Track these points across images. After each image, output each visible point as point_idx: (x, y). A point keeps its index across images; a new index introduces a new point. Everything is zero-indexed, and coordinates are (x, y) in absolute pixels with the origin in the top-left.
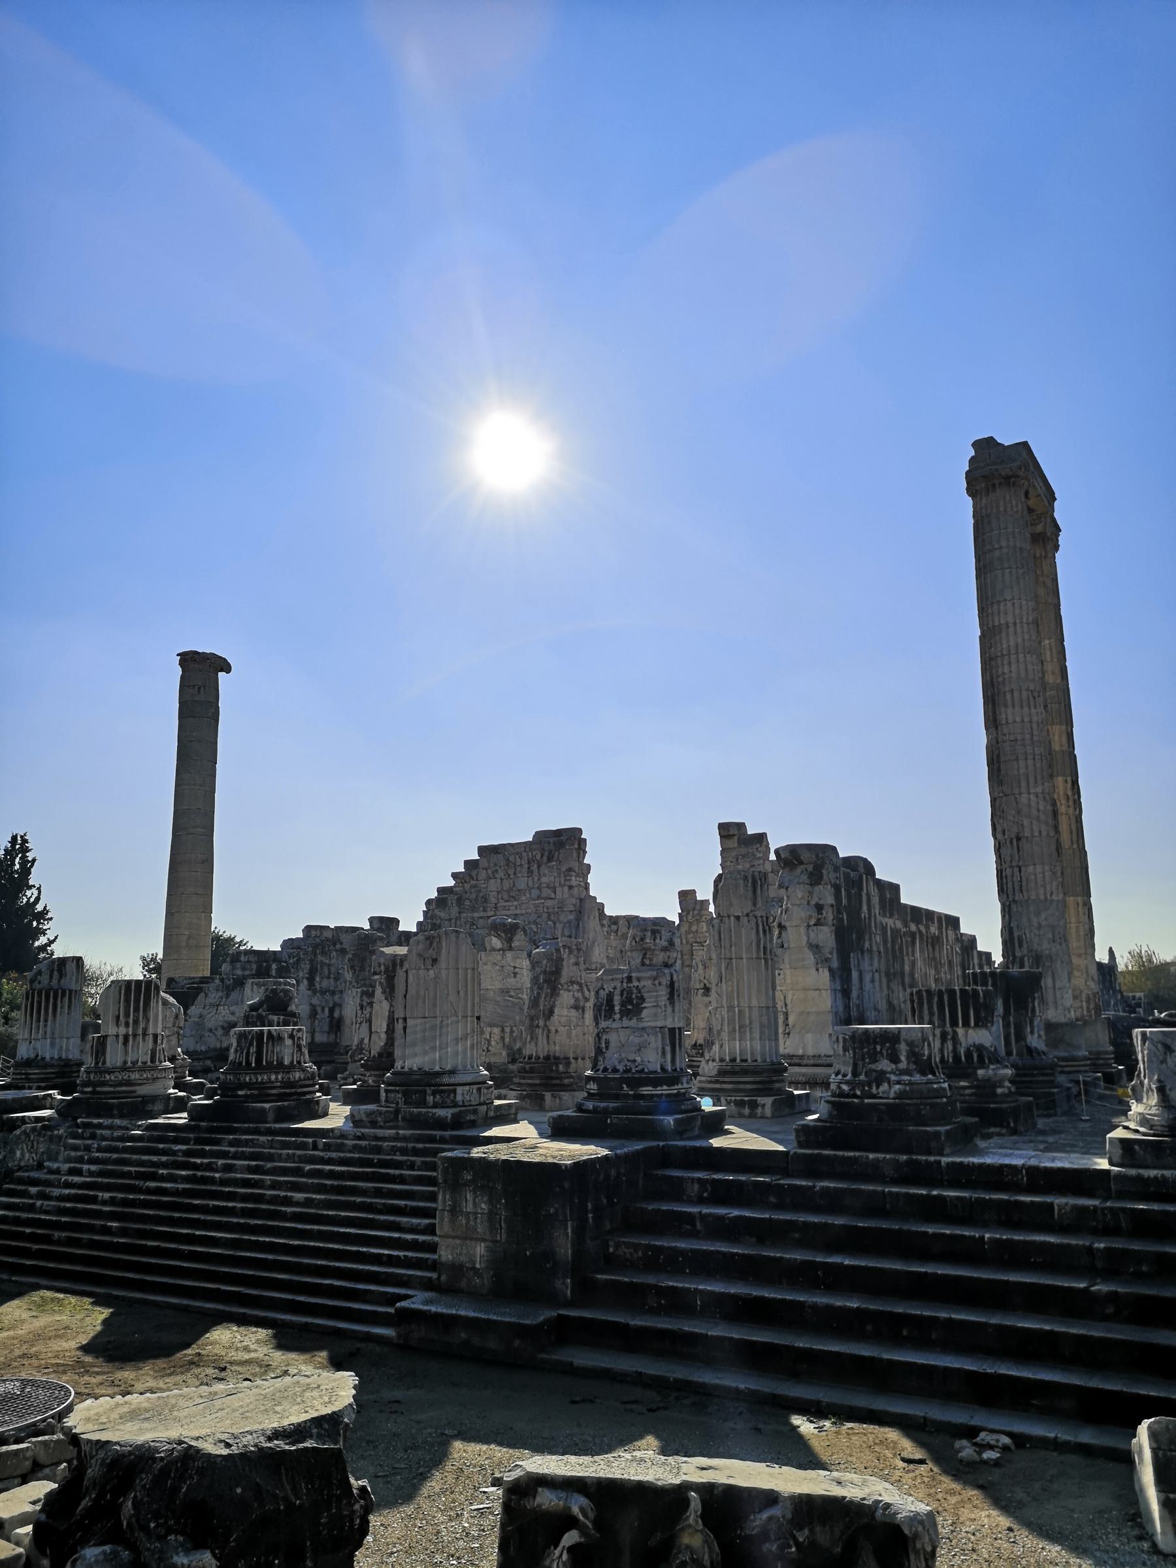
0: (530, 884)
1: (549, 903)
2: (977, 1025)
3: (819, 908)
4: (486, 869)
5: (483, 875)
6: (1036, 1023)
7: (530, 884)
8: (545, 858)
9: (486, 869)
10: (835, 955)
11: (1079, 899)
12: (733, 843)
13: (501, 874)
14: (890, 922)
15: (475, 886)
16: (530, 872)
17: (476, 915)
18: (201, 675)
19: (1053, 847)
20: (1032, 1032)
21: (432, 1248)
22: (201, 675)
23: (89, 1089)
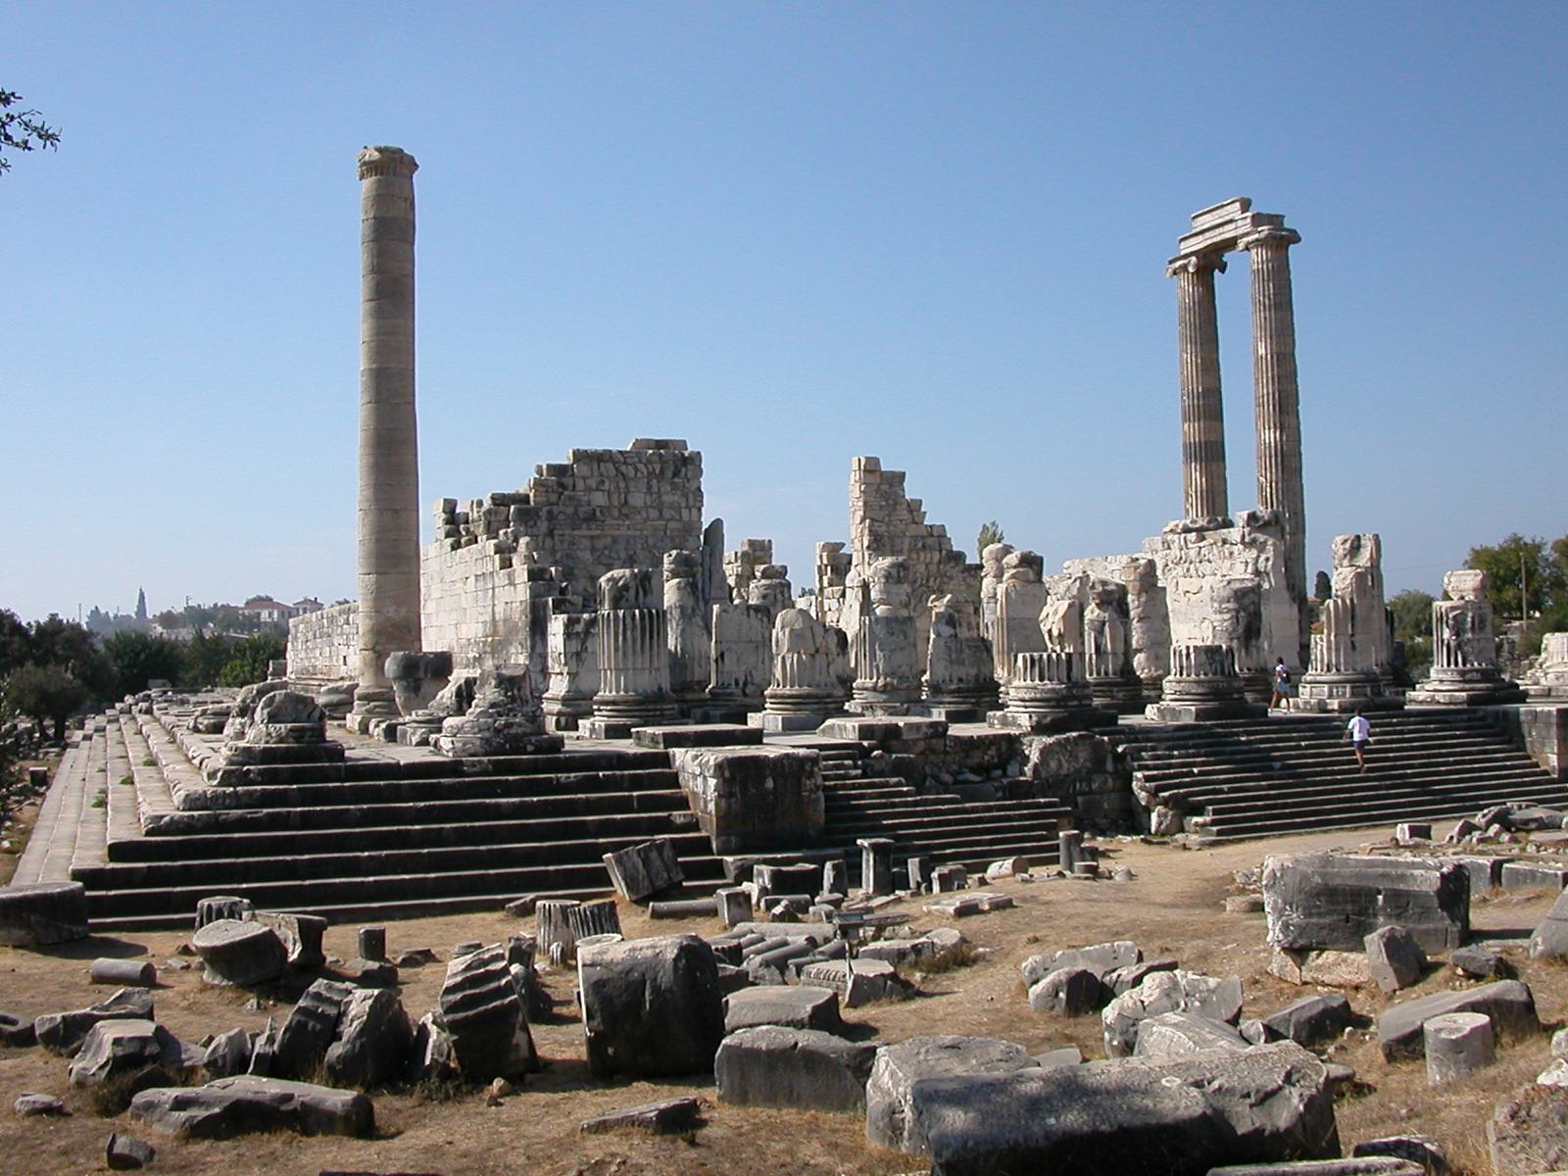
0: (649, 503)
1: (673, 525)
4: (584, 478)
5: (580, 485)
7: (649, 503)
8: (669, 473)
9: (584, 478)
12: (875, 479)
13: (606, 487)
15: (570, 498)
16: (649, 487)
17: (576, 533)
21: (1537, 766)
23: (1075, 703)
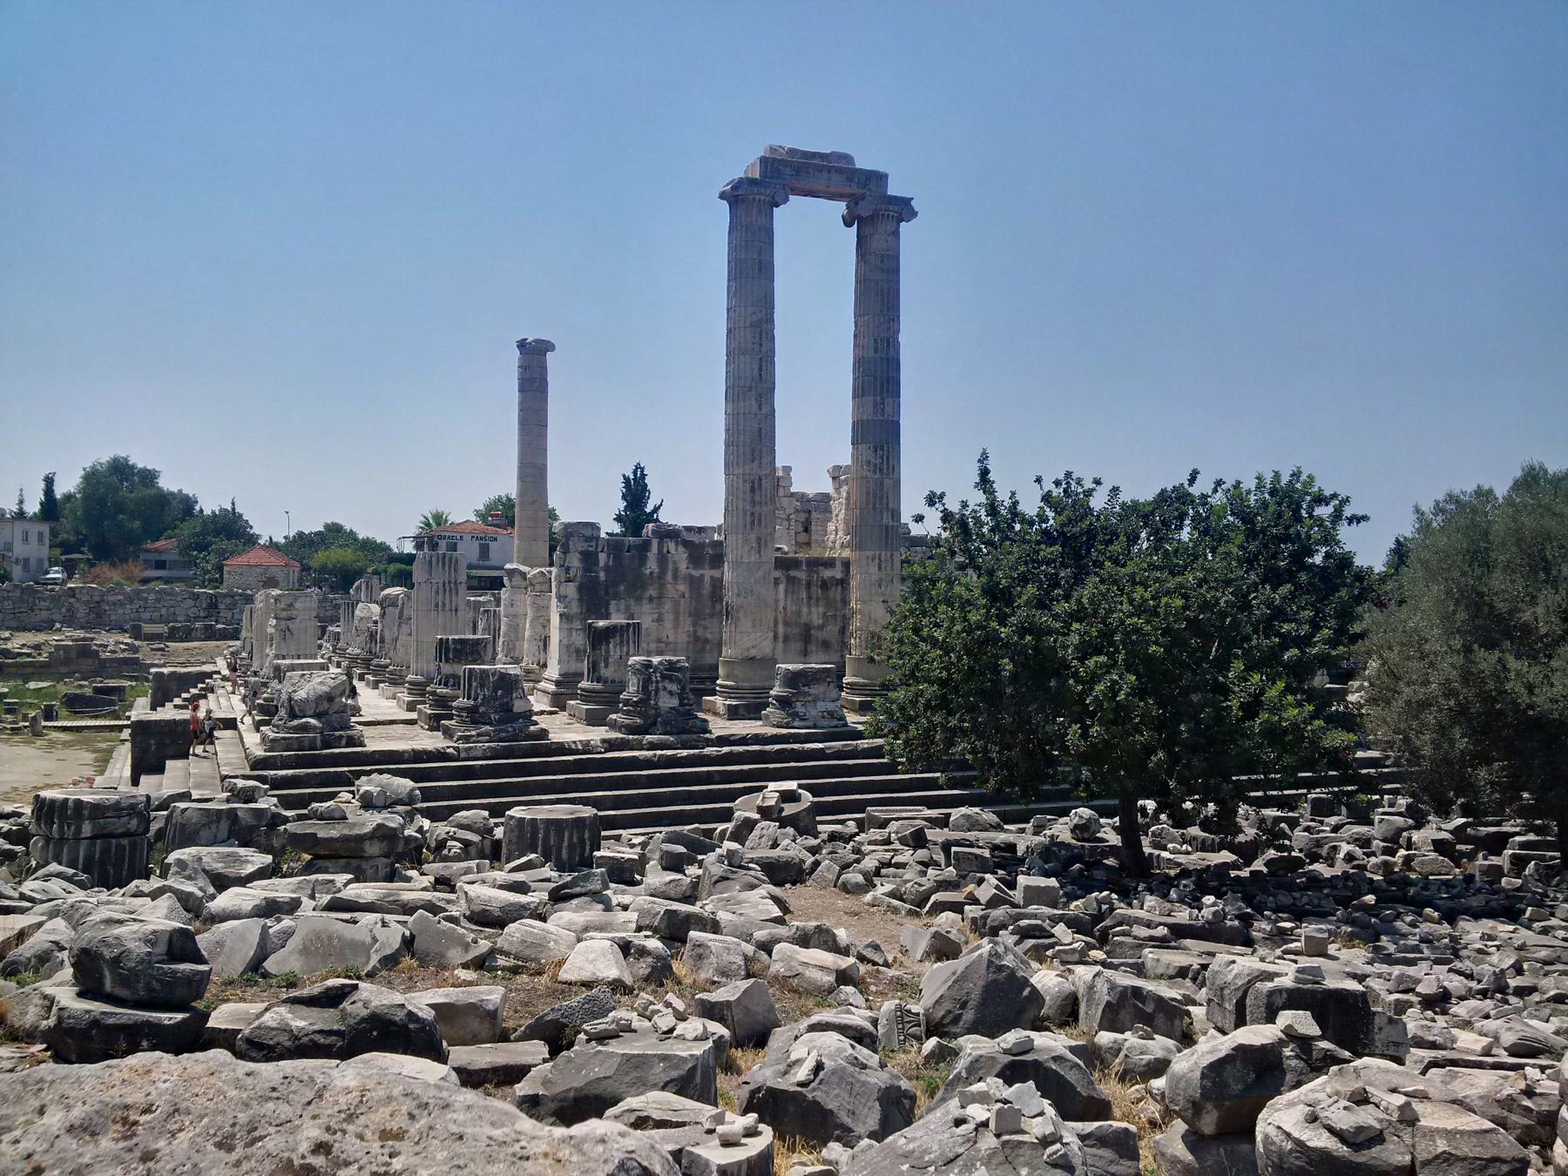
2: (447, 661)
3: (568, 570)
6: (611, 660)
10: (575, 604)
11: (870, 553)
14: (708, 574)
18: (534, 356)
19: (748, 519)
20: (606, 666)
22: (534, 356)
